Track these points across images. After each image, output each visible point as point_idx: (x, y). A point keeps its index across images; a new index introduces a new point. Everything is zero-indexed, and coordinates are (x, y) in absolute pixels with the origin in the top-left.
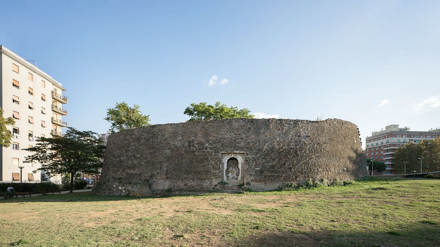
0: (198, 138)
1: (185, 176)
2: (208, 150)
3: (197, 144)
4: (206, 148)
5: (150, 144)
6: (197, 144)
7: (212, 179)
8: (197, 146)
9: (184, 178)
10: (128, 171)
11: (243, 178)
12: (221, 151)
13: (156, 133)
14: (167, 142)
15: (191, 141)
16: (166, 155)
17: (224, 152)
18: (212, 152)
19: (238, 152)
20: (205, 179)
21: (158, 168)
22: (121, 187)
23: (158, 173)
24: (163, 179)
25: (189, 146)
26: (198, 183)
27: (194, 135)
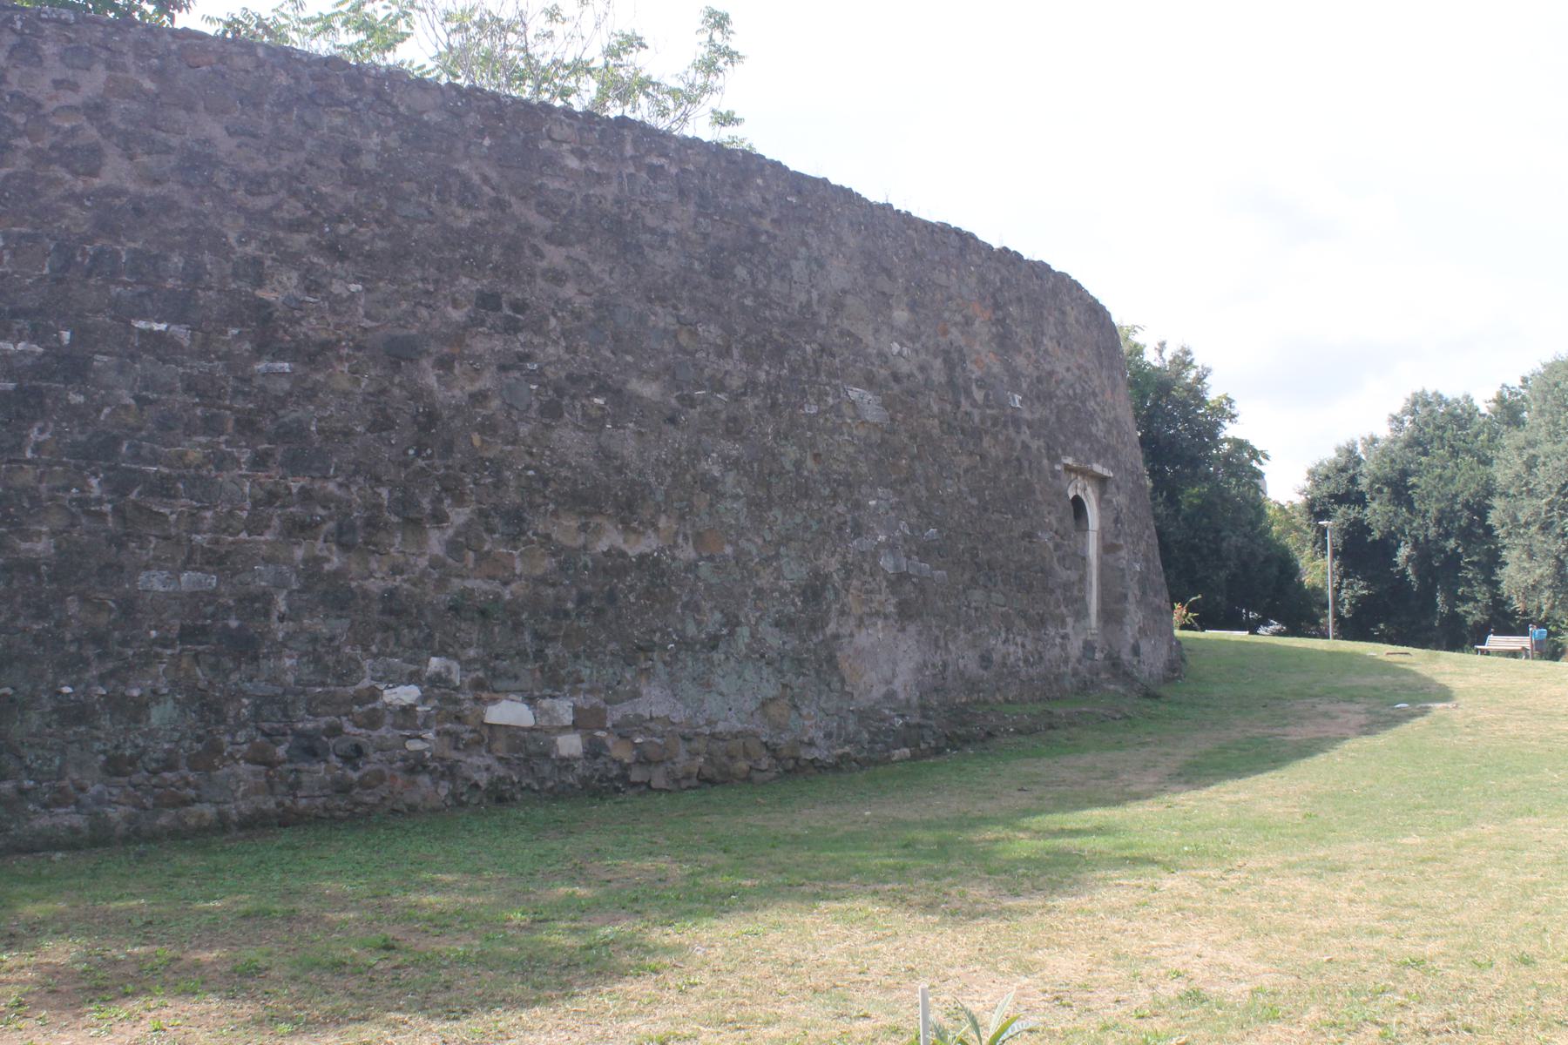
0: (977, 347)
1: (977, 595)
2: (1023, 437)
3: (981, 382)
4: (1016, 422)
5: (743, 308)
6: (981, 382)
7: (1063, 623)
8: (979, 395)
9: (976, 609)
10: (566, 530)
11: (1111, 616)
12: (1065, 453)
13: (766, 224)
14: (846, 324)
15: (955, 356)
16: (862, 432)
17: (1069, 461)
18: (1039, 449)
19: (1098, 468)
20: (1040, 623)
21: (840, 529)
22: (530, 701)
23: (848, 570)
24: (886, 617)
25: (951, 382)
26: (1029, 647)
27: (958, 318)
